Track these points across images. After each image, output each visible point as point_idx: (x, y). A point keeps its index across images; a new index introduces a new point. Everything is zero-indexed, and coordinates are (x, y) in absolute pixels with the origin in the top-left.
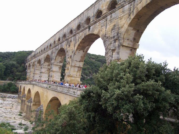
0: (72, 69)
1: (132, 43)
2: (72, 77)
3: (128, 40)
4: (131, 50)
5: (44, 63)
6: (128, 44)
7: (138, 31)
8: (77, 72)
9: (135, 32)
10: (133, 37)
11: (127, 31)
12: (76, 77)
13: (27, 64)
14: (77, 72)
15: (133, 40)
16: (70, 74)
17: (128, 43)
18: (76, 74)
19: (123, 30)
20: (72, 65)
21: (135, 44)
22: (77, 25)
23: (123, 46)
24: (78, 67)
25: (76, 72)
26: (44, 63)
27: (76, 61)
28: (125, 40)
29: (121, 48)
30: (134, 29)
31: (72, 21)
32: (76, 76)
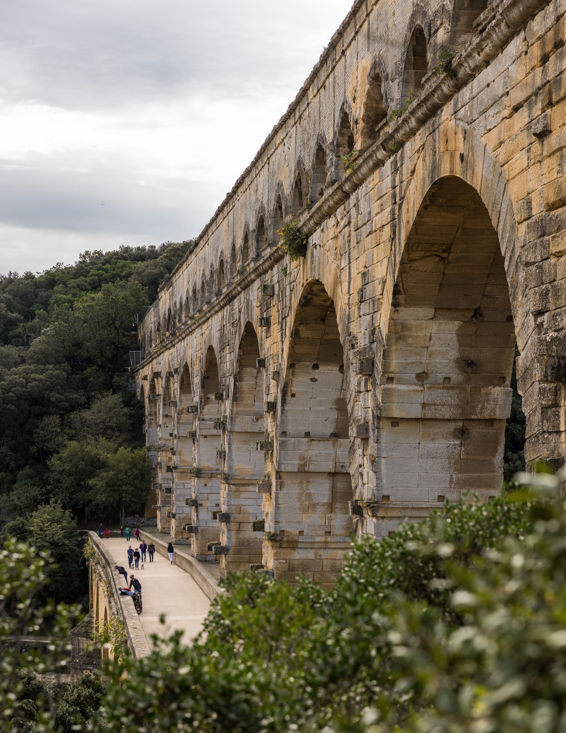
0: (292, 489)
1: (451, 392)
2: (293, 545)
3: (422, 377)
4: (462, 433)
5: (205, 400)
6: (424, 405)
7: (477, 313)
8: (332, 510)
9: (458, 323)
10: (454, 354)
11: (399, 332)
12: (325, 546)
13: (139, 379)
14: (332, 510)
15: (463, 371)
16: (284, 526)
17: (420, 398)
18: (321, 521)
19: (383, 320)
20: (283, 468)
21: (476, 390)
22: (293, 169)
23: (395, 422)
24: (333, 475)
25: (319, 509)
26: (205, 400)
27: (307, 435)
28: (400, 382)
29: (387, 433)
30: (442, 310)
31: (276, 131)
32: (322, 539)
